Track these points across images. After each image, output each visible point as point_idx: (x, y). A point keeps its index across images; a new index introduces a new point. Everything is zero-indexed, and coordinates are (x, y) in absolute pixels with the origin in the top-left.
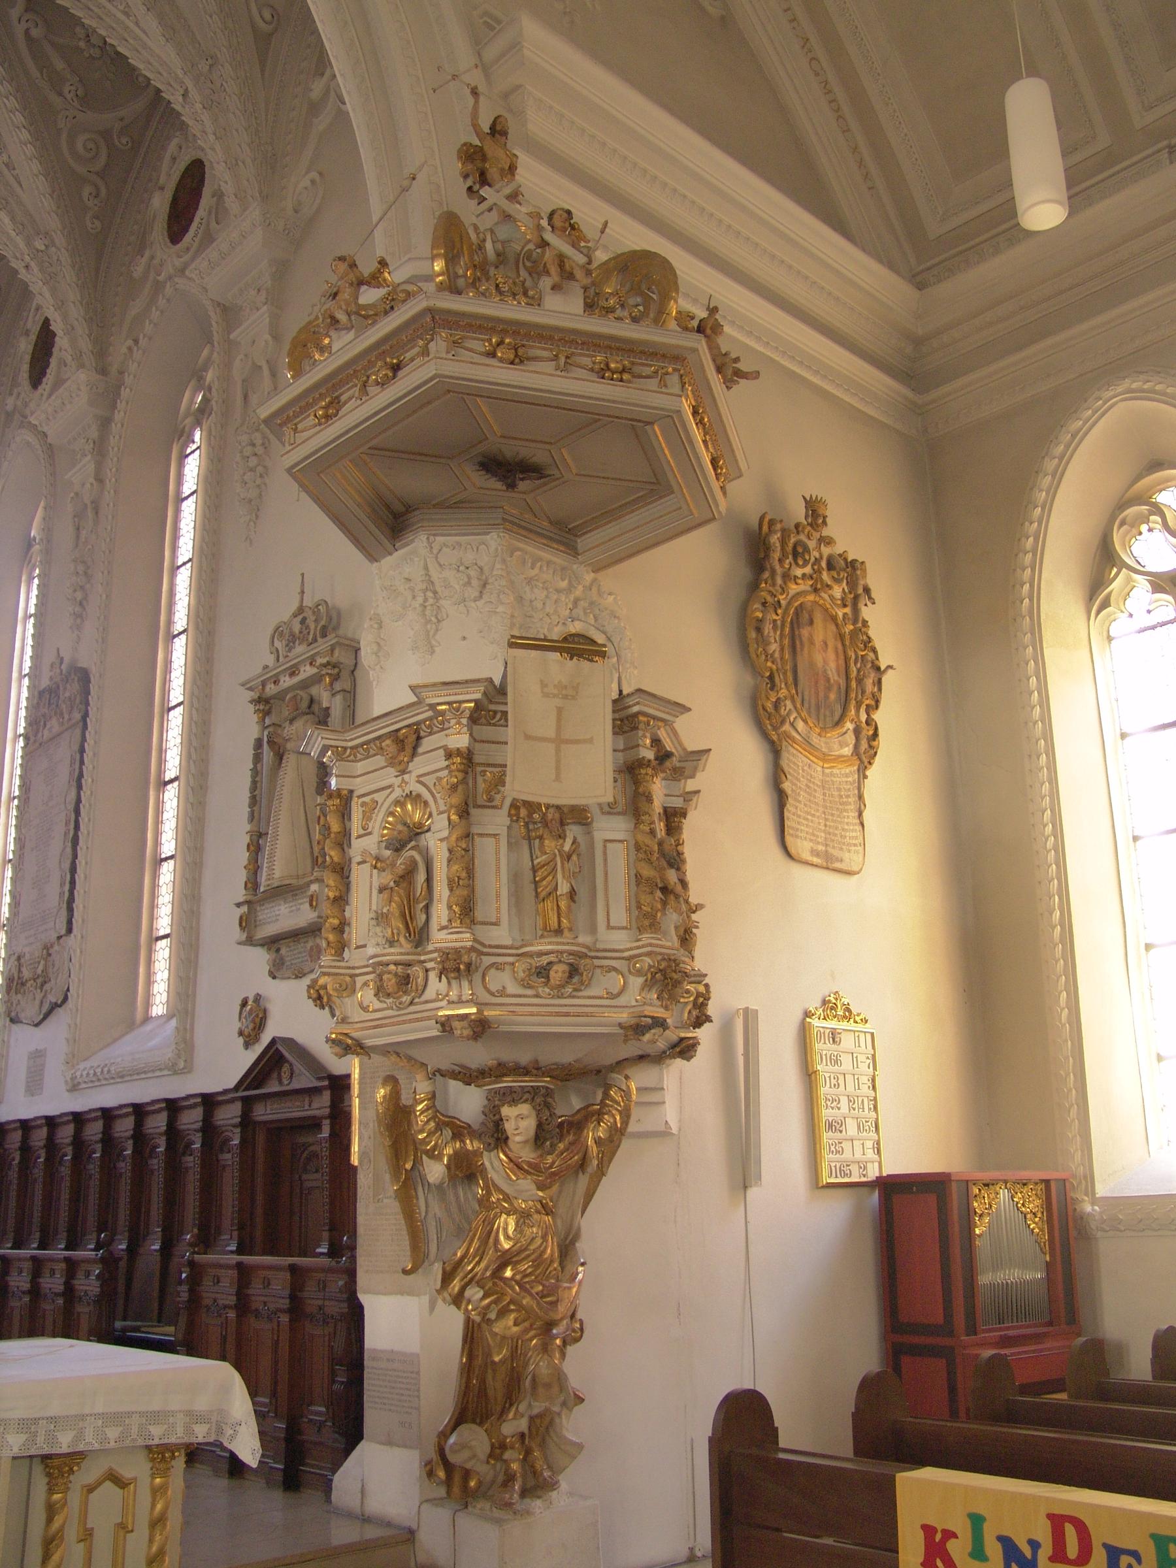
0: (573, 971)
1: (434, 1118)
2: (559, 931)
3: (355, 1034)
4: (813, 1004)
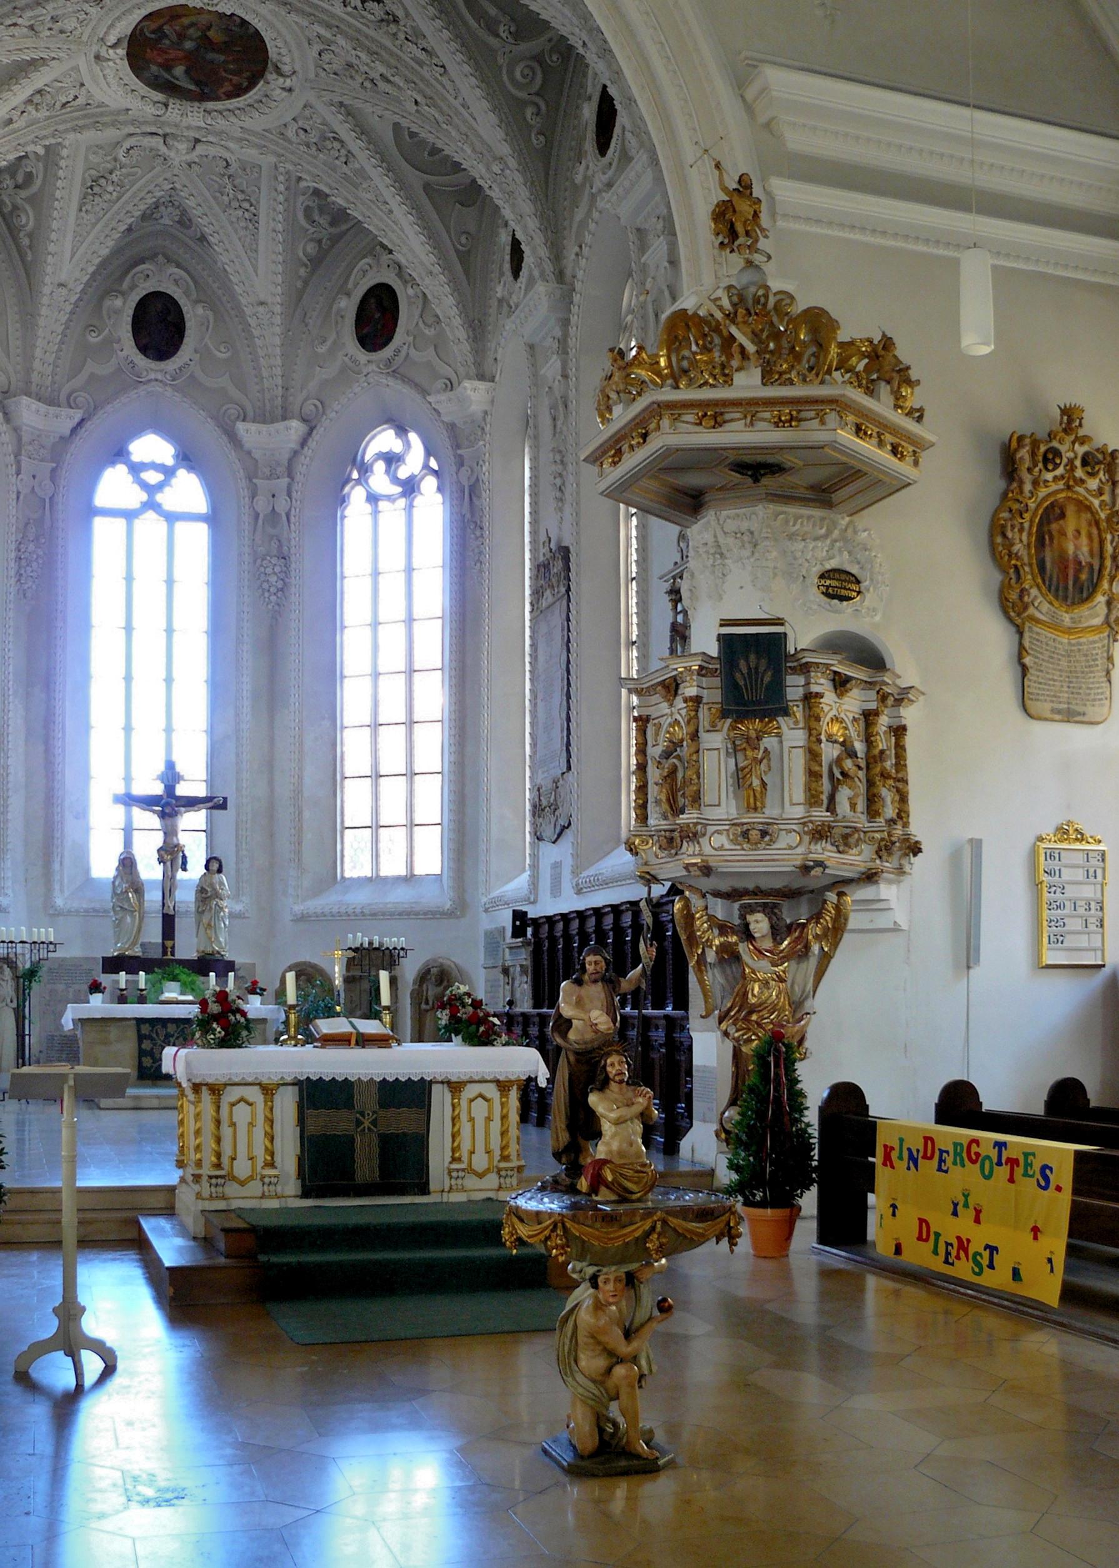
0: (764, 833)
1: (709, 920)
2: (755, 809)
3: (652, 872)
4: (1048, 830)
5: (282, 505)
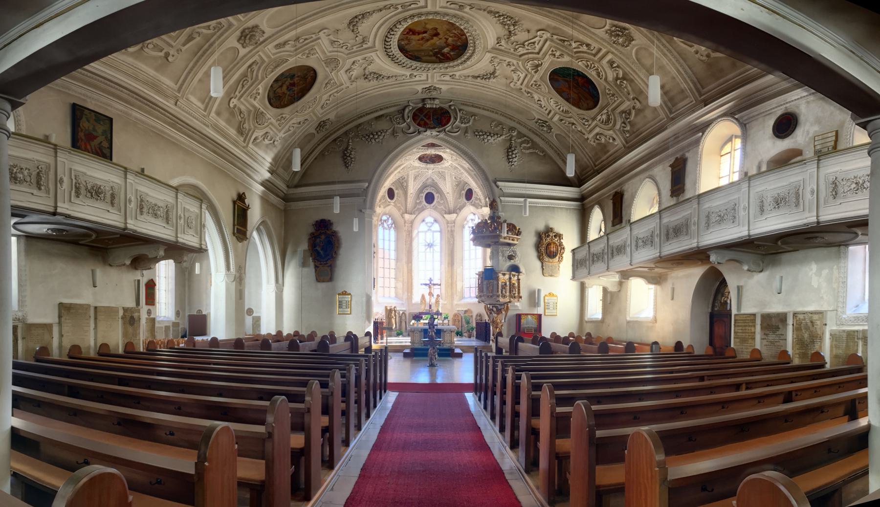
5: (453, 229)
